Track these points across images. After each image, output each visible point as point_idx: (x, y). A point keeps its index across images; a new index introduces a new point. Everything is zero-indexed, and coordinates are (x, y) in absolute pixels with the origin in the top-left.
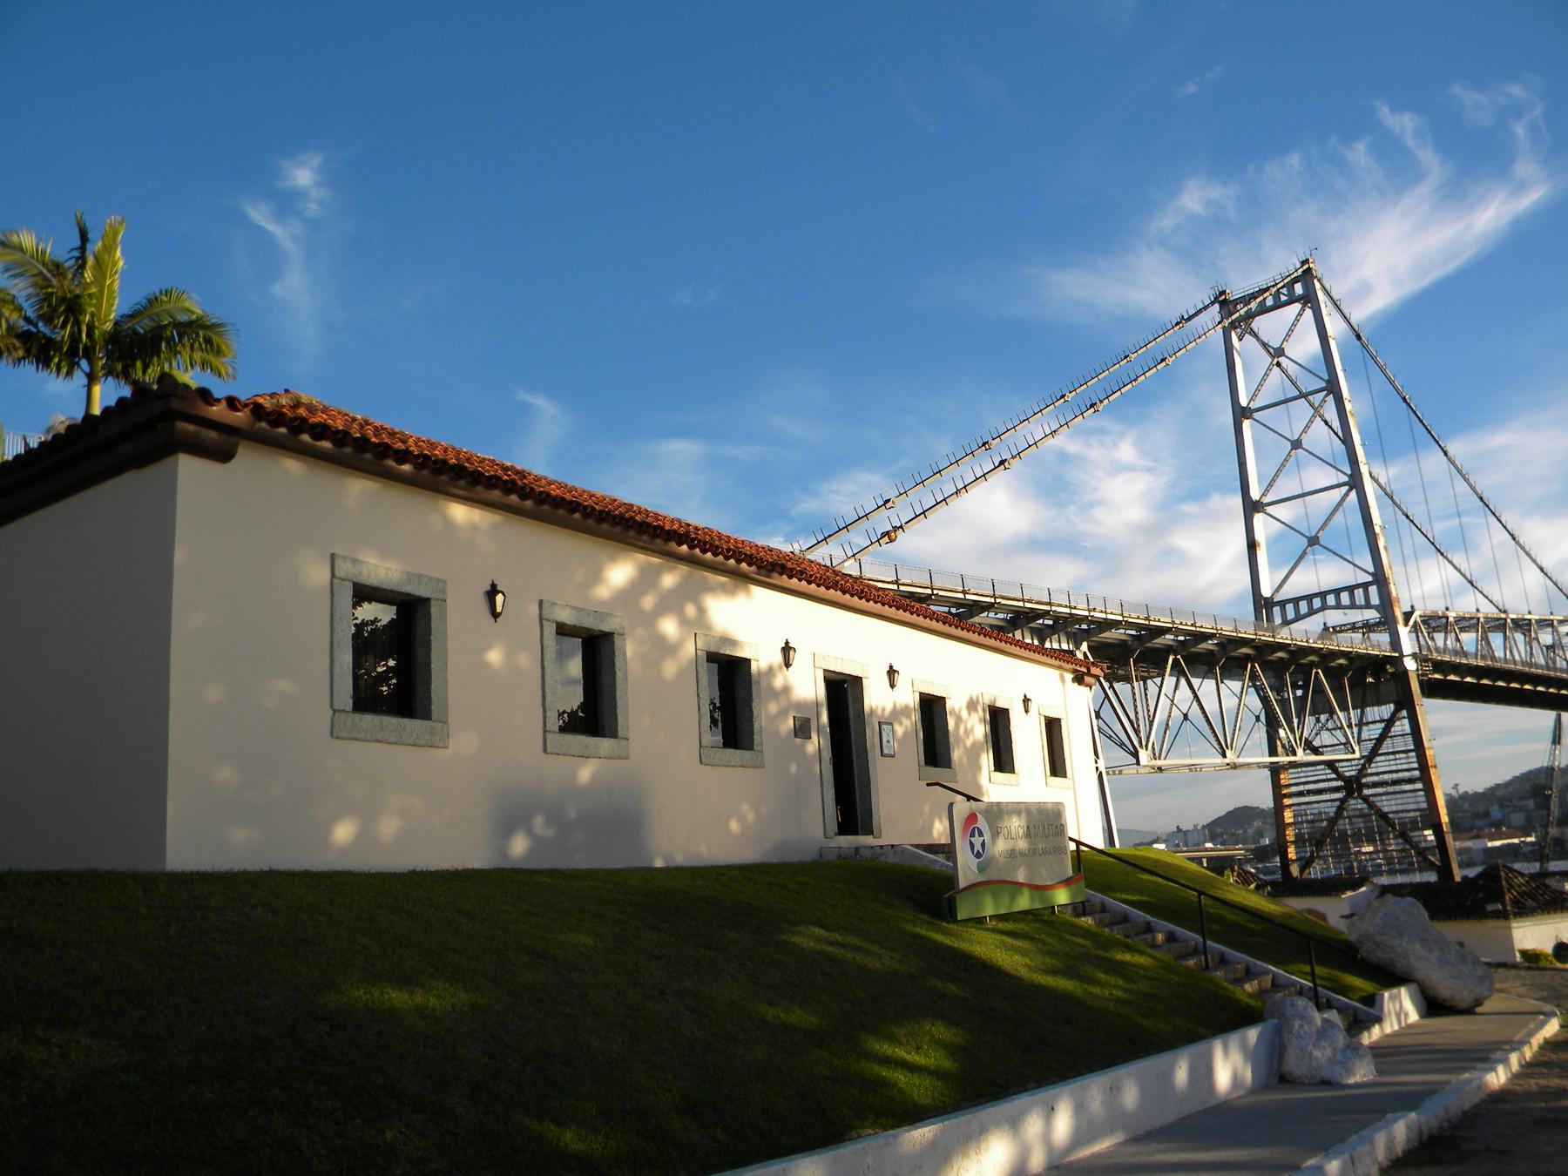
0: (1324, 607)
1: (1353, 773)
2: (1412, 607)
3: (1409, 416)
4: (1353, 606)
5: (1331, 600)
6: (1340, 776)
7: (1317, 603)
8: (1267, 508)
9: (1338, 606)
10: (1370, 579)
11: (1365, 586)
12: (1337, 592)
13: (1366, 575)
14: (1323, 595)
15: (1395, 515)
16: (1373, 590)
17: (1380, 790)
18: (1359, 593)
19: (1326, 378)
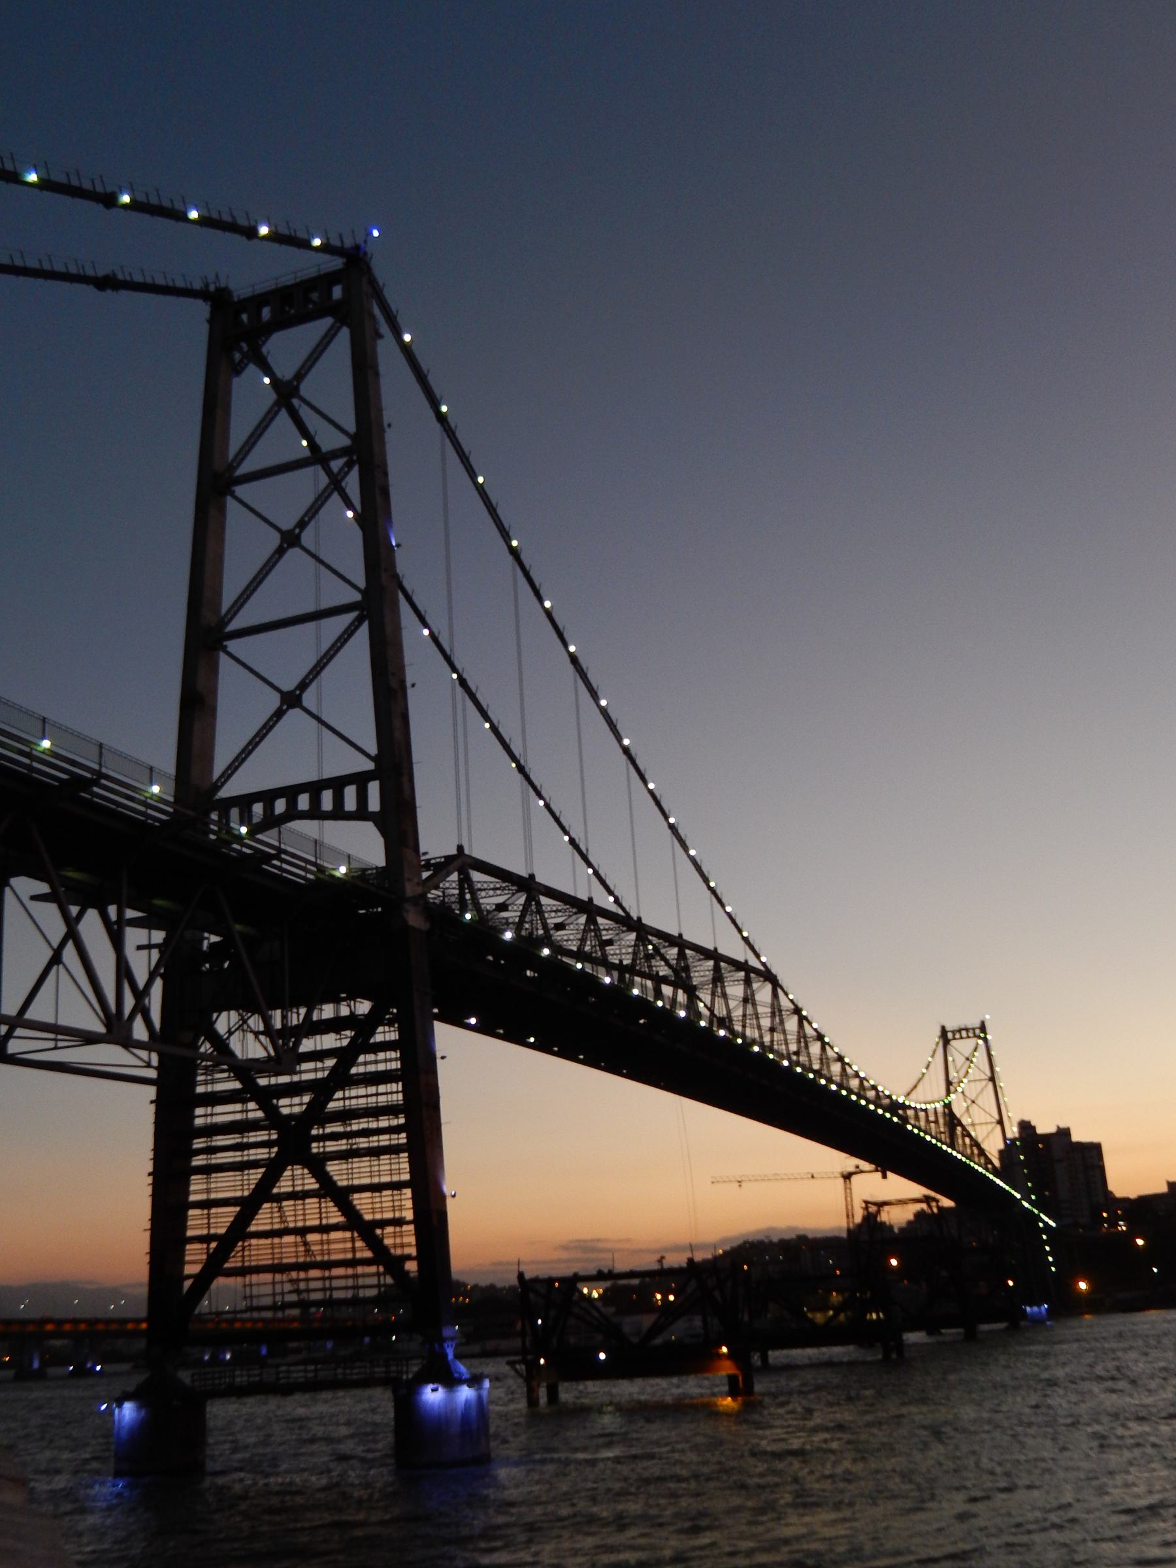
0: (293, 814)
1: (296, 1110)
2: (460, 848)
3: (515, 580)
4: (339, 813)
5: (303, 802)
6: (274, 1119)
7: (280, 806)
9: (315, 813)
10: (370, 766)
11: (360, 780)
12: (314, 788)
14: (291, 793)
15: (590, 886)
16: (374, 788)
17: (342, 1145)
18: (350, 793)
19: (351, 427)
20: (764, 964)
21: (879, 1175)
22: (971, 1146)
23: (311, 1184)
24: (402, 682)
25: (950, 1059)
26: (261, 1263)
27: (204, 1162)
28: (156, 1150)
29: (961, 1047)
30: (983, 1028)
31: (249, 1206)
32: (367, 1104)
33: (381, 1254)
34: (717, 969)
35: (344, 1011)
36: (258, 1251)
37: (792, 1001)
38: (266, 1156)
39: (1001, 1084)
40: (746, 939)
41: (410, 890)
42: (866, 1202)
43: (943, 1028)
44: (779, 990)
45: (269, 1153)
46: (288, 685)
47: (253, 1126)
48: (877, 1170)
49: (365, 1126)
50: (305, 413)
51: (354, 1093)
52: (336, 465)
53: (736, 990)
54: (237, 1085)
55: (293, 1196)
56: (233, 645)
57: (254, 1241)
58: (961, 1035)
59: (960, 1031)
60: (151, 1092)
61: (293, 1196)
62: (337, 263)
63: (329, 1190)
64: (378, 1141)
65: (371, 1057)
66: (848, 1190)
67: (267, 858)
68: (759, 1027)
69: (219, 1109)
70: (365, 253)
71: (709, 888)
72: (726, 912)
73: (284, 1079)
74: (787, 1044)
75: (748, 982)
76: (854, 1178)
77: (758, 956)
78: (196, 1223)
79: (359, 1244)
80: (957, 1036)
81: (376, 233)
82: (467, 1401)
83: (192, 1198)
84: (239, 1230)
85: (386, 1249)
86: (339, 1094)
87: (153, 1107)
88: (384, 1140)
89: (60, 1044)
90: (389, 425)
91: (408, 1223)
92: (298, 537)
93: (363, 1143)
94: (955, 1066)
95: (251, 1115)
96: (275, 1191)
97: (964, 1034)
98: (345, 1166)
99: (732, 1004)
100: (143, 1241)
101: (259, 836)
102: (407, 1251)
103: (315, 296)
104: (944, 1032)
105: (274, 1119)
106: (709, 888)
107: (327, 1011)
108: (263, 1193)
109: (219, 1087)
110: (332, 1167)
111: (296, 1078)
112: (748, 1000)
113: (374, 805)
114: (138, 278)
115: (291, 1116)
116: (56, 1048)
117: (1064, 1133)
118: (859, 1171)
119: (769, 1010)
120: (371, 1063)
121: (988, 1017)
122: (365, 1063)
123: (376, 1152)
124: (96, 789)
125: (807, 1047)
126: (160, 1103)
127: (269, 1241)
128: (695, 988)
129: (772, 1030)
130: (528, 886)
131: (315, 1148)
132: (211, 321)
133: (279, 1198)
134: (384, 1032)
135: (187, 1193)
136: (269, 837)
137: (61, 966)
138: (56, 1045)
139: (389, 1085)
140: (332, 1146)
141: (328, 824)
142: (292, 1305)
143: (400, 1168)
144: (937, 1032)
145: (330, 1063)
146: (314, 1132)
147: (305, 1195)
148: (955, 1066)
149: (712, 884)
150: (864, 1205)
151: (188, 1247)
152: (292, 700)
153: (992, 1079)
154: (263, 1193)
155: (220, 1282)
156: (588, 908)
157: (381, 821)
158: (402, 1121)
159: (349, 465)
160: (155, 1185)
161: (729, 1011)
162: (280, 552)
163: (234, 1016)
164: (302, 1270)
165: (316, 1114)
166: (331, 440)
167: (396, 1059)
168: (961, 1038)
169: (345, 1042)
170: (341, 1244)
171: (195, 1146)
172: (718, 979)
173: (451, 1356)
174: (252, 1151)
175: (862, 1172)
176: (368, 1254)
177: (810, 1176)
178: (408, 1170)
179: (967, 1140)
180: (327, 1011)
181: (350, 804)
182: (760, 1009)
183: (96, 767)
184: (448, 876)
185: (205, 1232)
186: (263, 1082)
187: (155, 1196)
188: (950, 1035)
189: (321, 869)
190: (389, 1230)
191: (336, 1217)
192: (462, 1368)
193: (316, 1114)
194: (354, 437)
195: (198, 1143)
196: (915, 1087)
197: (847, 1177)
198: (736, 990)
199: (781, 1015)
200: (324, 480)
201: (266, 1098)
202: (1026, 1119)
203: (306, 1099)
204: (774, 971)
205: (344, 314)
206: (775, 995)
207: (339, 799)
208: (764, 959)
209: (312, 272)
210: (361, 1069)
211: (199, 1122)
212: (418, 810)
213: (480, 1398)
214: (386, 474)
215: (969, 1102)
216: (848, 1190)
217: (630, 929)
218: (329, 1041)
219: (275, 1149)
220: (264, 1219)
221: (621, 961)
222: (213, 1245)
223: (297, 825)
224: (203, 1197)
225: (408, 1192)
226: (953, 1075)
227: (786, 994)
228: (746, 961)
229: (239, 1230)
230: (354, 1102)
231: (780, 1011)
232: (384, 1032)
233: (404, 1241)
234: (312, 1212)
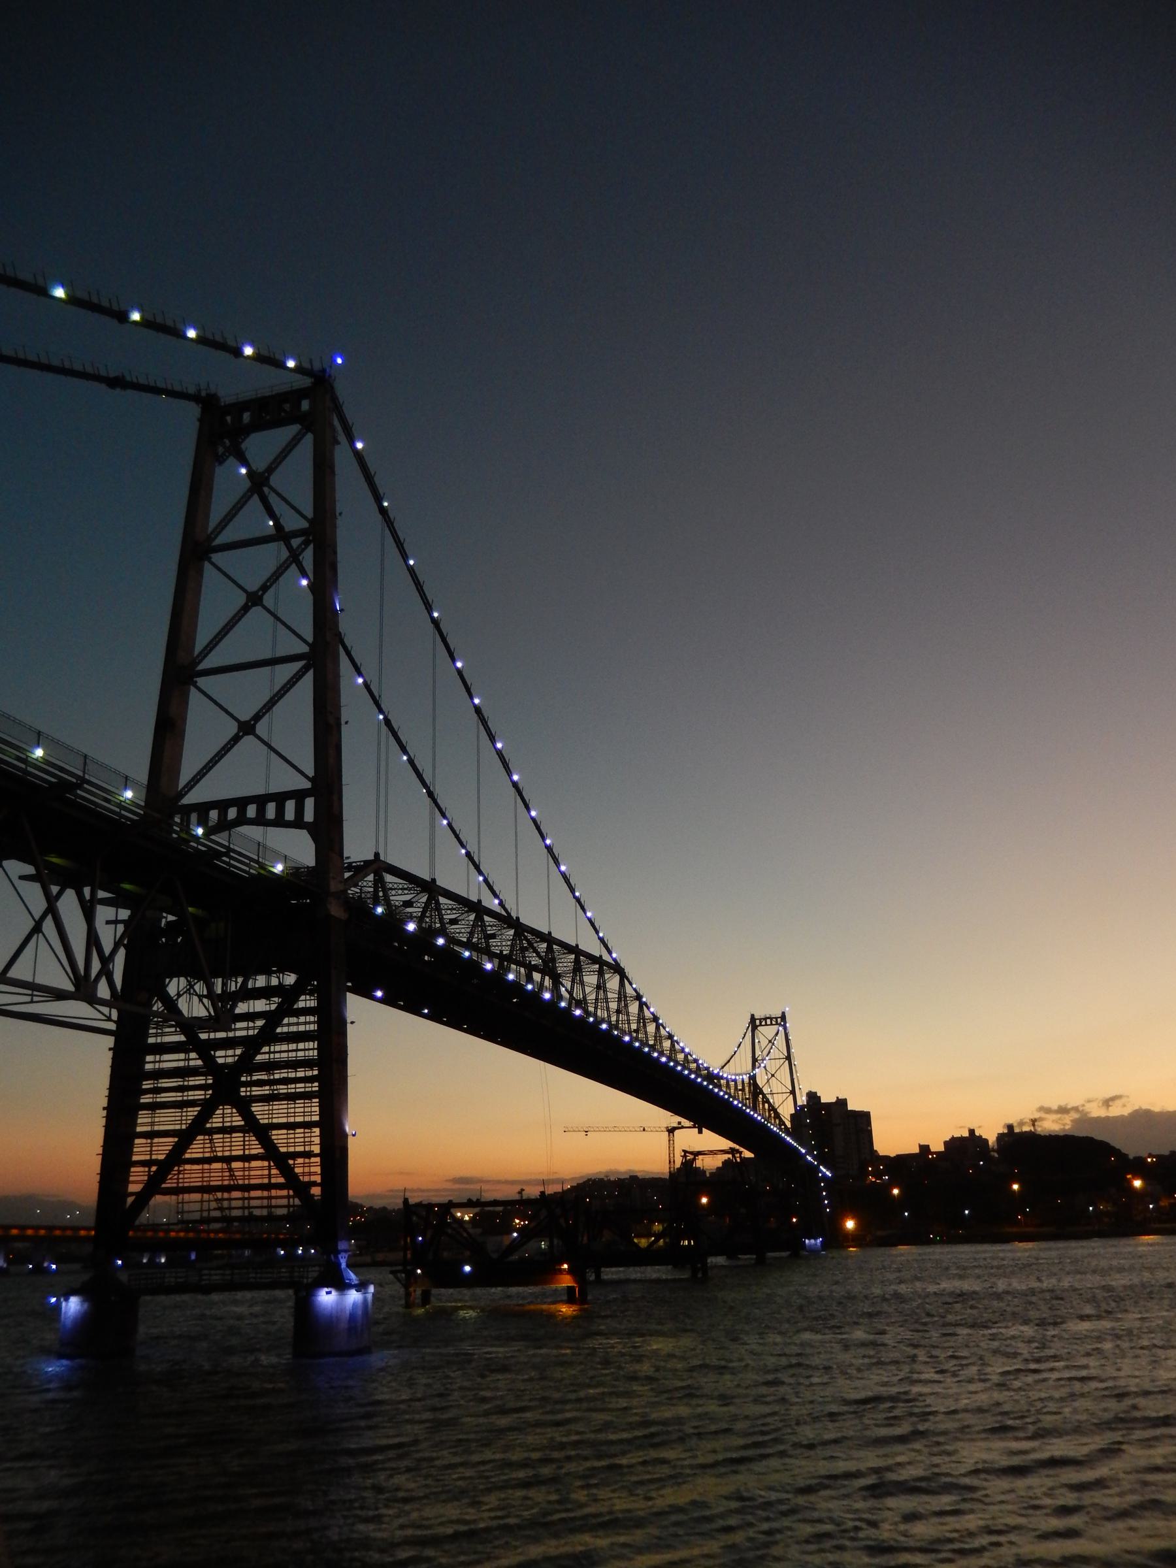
0: (242, 820)
1: (230, 1060)
2: (377, 855)
4: (279, 822)
5: (251, 811)
6: (210, 1066)
7: (232, 813)
8: (197, 679)
9: (260, 820)
10: (308, 785)
11: (299, 796)
12: (261, 801)
13: (305, 780)
14: (241, 803)
16: (309, 803)
17: (265, 1090)
18: (290, 806)
19: (310, 513)
20: (614, 960)
21: (696, 1130)
22: (769, 1110)
23: (238, 1121)
24: (338, 719)
25: (757, 1041)
26: (192, 1184)
27: (151, 1100)
28: (111, 1089)
29: (767, 1032)
30: (783, 1017)
31: (185, 1138)
32: (288, 1057)
33: (292, 1181)
34: (577, 962)
35: (274, 982)
36: (191, 1175)
37: (635, 990)
38: (203, 1097)
39: (796, 1062)
40: (602, 940)
41: (334, 886)
42: (685, 1151)
43: (753, 1016)
44: (625, 980)
45: (205, 1095)
46: (245, 716)
47: (194, 1072)
48: (694, 1127)
49: (285, 1075)
50: (273, 499)
51: (278, 1048)
52: (295, 542)
53: (591, 979)
54: (182, 1038)
55: (223, 1130)
56: (202, 681)
57: (187, 1167)
58: (766, 1022)
59: (765, 1019)
60: (110, 1041)
61: (223, 1130)
62: (307, 382)
63: (253, 1126)
64: (295, 1088)
65: (294, 1020)
66: (671, 1141)
67: (218, 855)
68: (608, 1009)
69: (166, 1057)
70: (330, 376)
71: (575, 897)
72: (587, 917)
73: (221, 1035)
74: (629, 1023)
75: (601, 973)
76: (677, 1132)
77: (610, 952)
78: (140, 1150)
79: (274, 1172)
80: (763, 1023)
81: (339, 361)
82: (355, 1304)
83: (139, 1129)
84: (176, 1157)
85: (296, 1176)
86: (266, 1049)
87: (111, 1054)
88: (300, 1087)
89: (35, 999)
90: (340, 514)
91: (316, 1155)
92: (261, 598)
93: (282, 1089)
94: (760, 1047)
95: (192, 1063)
96: (208, 1125)
97: (769, 1021)
98: (266, 1108)
99: (588, 990)
100: (95, 1163)
101: (213, 837)
102: (313, 1178)
103: (287, 406)
104: (753, 1019)
105: (210, 1066)
106: (575, 897)
107: (261, 981)
108: (198, 1127)
109: (167, 1039)
110: (256, 1108)
111: (231, 1034)
112: (601, 987)
113: (309, 816)
114: (142, 381)
115: (225, 1065)
116: (32, 1002)
117: (842, 1103)
118: (680, 1127)
119: (617, 996)
120: (293, 1024)
121: (787, 1009)
122: (289, 1025)
123: (292, 1097)
124: (79, 792)
125: (645, 1026)
126: (115, 1050)
127: (200, 1167)
128: (559, 976)
129: (618, 1012)
130: (430, 888)
131: (243, 1091)
132: (200, 420)
133: (211, 1132)
134: (306, 1000)
135: (135, 1124)
136: (221, 838)
137: (40, 934)
138: (32, 999)
139: (307, 1043)
140: (257, 1091)
141: (271, 830)
142: (216, 1220)
143: (312, 1111)
144: (749, 1017)
145: (260, 1023)
146: (243, 1079)
147: (232, 1130)
148: (760, 1047)
149: (577, 894)
150: (683, 1154)
151: (133, 1169)
152: (247, 728)
153: (788, 1058)
154: (198, 1127)
155: (158, 1199)
156: (477, 908)
157: (314, 830)
158: (316, 1073)
159: (306, 543)
160: (108, 1117)
161: (585, 997)
162: (245, 609)
163: (183, 981)
164: (226, 1192)
165: (246, 1064)
166: (293, 523)
167: (314, 1023)
168: (766, 1025)
169: (273, 1007)
170: (260, 1170)
171: (144, 1087)
172: (577, 969)
173: (343, 1265)
174: (191, 1093)
175: (683, 1127)
176: (281, 1180)
177: (642, 1129)
178: (318, 1113)
179: (766, 1105)
180: (261, 981)
181: (290, 814)
182: (610, 995)
183: (80, 774)
184: (366, 877)
185: (148, 1157)
186: (203, 1036)
187: (107, 1127)
188: (758, 1022)
189: (262, 866)
190: (300, 1160)
191: (257, 1150)
192: (352, 1276)
193: (246, 1064)
194: (311, 522)
195: (147, 1085)
196: (729, 1061)
197: (671, 1131)
198: (591, 979)
199: (625, 1000)
200: (285, 554)
201: (205, 1050)
202: (813, 1091)
203: (238, 1052)
204: (622, 965)
205: (308, 423)
206: (622, 984)
207: (280, 810)
208: (614, 955)
209: (285, 388)
210: (285, 1029)
211: (148, 1067)
212: (345, 823)
213: (365, 1300)
214: (335, 553)
215: (770, 1076)
216: (671, 1141)
217: (510, 927)
218: (260, 1005)
219: (210, 1092)
220: (197, 1149)
221: (501, 951)
222: (154, 1168)
223: (245, 830)
224: (148, 1129)
225: (317, 1131)
226: (758, 1053)
227: (631, 984)
228: (601, 956)
229: (176, 1157)
230: (277, 1055)
231: (625, 997)
232: (306, 1000)
233: (311, 1170)
234: (237, 1144)
